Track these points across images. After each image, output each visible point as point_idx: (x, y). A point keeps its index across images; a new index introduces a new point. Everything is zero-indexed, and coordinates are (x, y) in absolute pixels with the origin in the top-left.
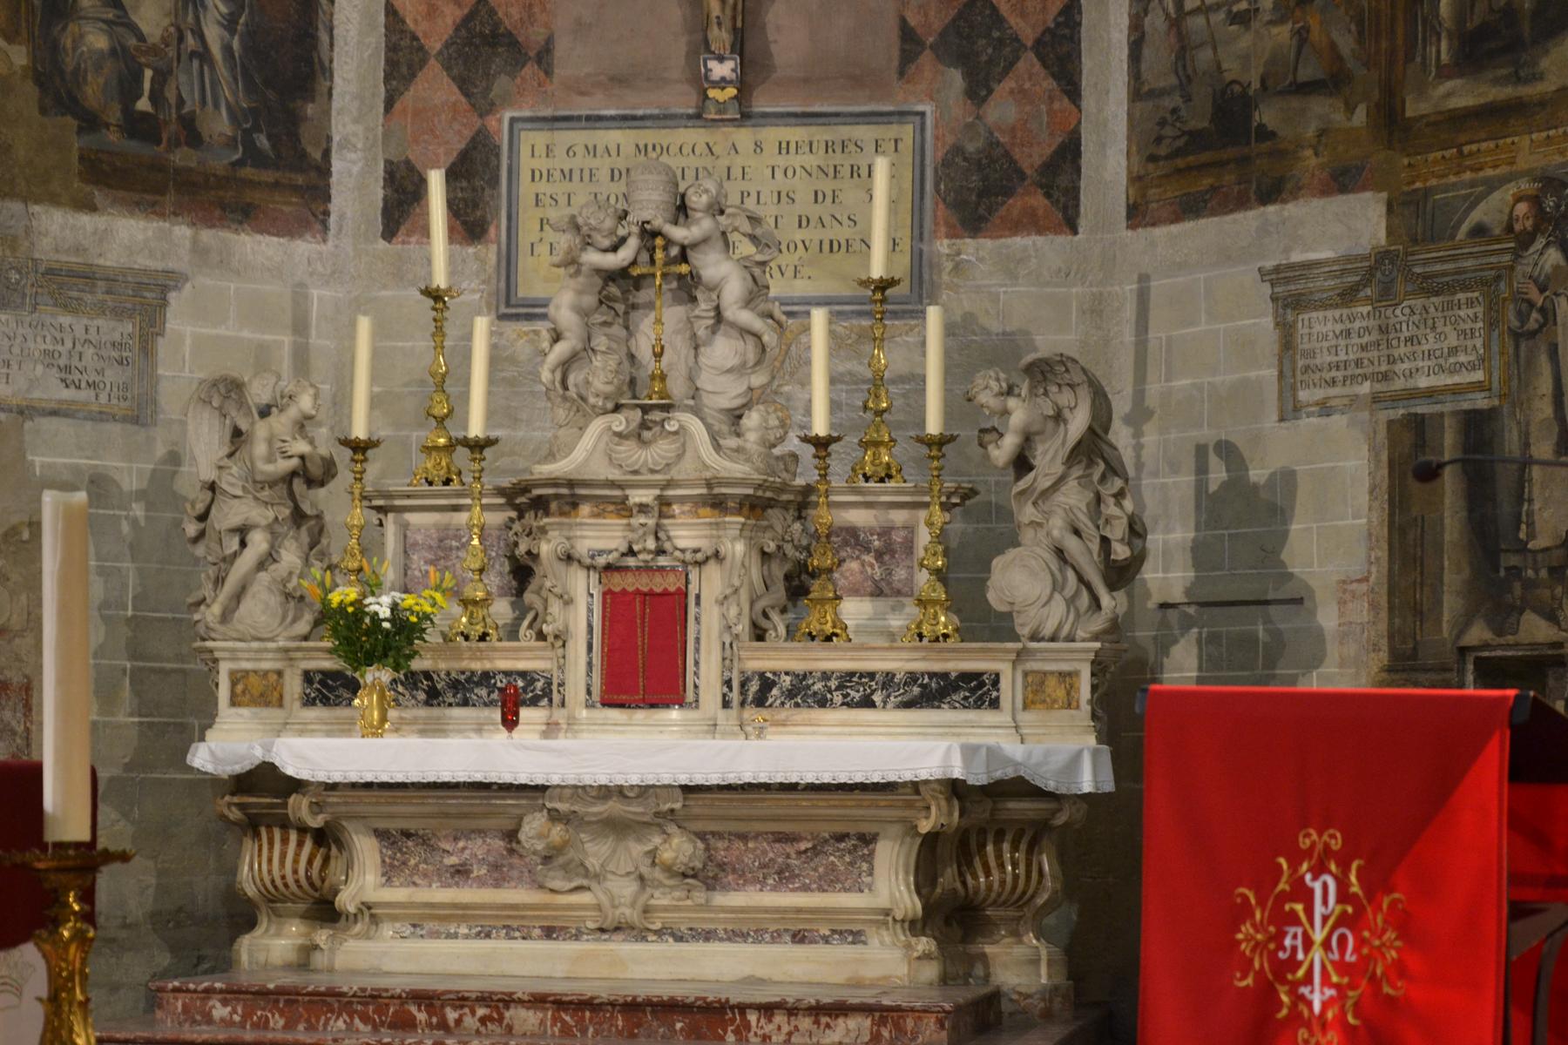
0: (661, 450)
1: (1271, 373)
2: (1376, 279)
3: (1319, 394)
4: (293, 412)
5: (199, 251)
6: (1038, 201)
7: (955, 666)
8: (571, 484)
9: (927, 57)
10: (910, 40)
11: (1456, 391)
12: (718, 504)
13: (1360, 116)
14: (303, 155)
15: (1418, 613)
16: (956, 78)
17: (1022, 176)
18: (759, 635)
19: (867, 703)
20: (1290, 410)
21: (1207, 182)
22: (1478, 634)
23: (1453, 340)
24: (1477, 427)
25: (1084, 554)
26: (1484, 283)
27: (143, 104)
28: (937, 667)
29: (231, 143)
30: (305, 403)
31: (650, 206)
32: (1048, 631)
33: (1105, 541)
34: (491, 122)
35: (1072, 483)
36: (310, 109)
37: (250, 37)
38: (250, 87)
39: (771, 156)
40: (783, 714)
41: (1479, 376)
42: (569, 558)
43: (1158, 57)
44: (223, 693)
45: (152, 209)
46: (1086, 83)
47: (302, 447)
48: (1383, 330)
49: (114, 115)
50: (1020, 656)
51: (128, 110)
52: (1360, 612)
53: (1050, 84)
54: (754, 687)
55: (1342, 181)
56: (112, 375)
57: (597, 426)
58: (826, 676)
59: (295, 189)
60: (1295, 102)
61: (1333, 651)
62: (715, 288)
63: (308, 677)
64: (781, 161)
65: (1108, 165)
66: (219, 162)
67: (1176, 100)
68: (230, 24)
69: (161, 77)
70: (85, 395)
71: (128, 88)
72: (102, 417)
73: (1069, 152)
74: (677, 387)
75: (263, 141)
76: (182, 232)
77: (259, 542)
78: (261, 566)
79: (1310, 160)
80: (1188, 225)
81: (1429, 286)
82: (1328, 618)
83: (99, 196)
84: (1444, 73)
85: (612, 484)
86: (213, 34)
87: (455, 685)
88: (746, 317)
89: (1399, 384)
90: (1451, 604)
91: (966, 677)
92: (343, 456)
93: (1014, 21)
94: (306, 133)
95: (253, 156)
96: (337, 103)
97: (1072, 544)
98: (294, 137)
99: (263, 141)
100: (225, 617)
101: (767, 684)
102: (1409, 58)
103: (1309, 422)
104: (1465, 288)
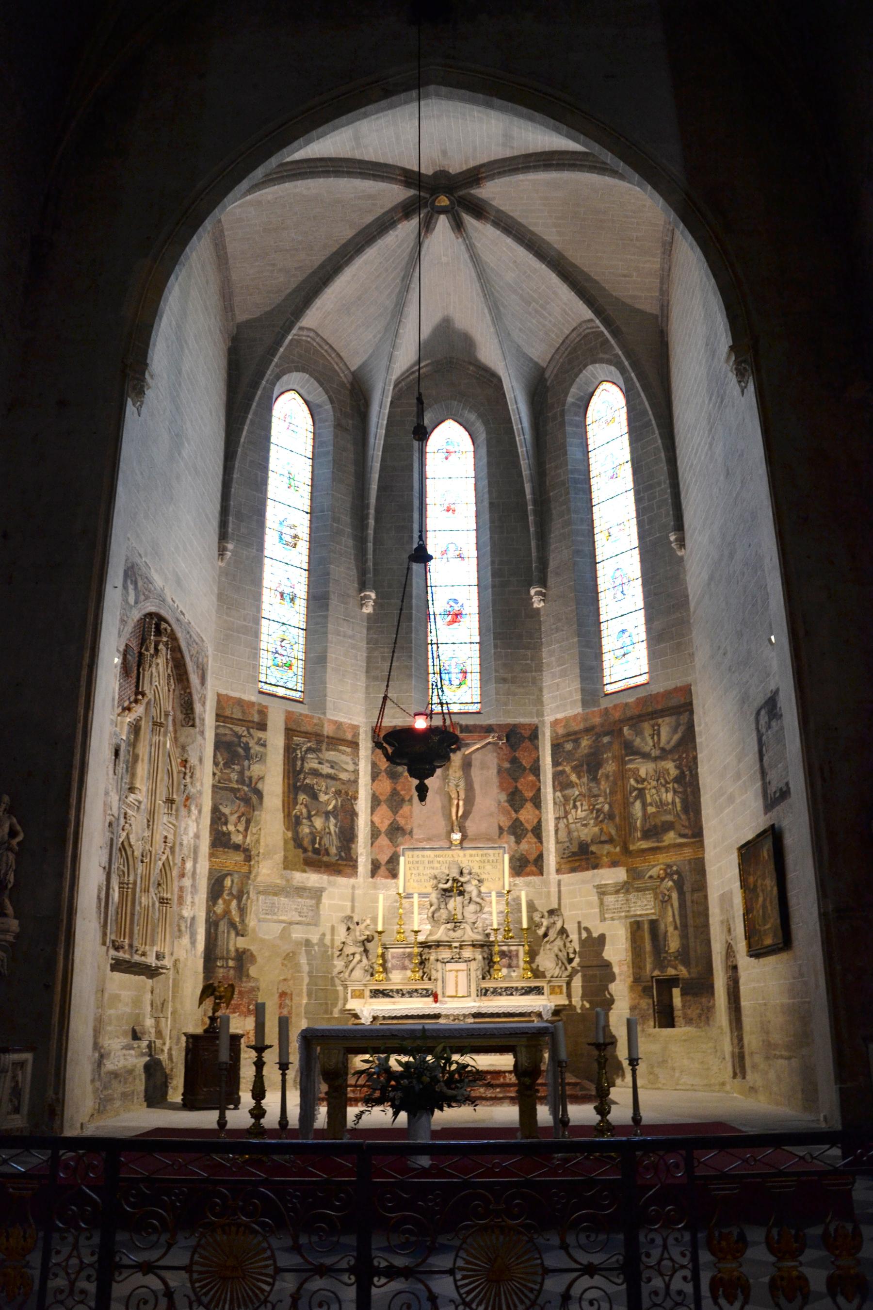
0: (459, 933)
1: (597, 910)
2: (625, 888)
3: (611, 915)
4: (365, 924)
5: (329, 882)
6: (534, 869)
7: (533, 985)
8: (438, 942)
9: (505, 833)
10: (500, 828)
11: (647, 915)
12: (474, 946)
13: (618, 849)
14: (352, 858)
15: (640, 968)
16: (512, 838)
17: (529, 862)
18: (484, 978)
19: (511, 994)
20: (603, 919)
21: (577, 864)
22: (656, 973)
23: (645, 903)
24: (654, 924)
25: (563, 955)
26: (653, 889)
27: (317, 846)
28: (529, 985)
29: (336, 855)
30: (368, 922)
31: (455, 874)
32: (555, 975)
33: (568, 953)
34: (398, 849)
35: (558, 939)
36: (353, 846)
37: (340, 828)
38: (340, 841)
39: (468, 857)
40: (491, 998)
41: (653, 911)
42: (437, 960)
43: (563, 834)
44: (349, 995)
45: (319, 872)
46: (544, 839)
47: (368, 933)
48: (627, 900)
49: (310, 848)
50: (550, 981)
51: (313, 847)
52: (625, 968)
53: (535, 840)
54: (484, 991)
55: (614, 864)
56: (310, 914)
57: (443, 927)
58: (501, 988)
59: (350, 866)
60: (600, 846)
61: (618, 978)
62: (469, 893)
63: (371, 991)
64: (471, 859)
65: (551, 860)
66: (334, 859)
67: (568, 844)
68: (336, 825)
69: (321, 839)
70: (304, 919)
71: (313, 842)
72: (308, 924)
73: (540, 857)
74: (459, 917)
75: (343, 854)
76: (325, 877)
77: (357, 957)
78: (358, 963)
79: (605, 859)
80: (573, 874)
81: (638, 890)
82: (616, 970)
83: (307, 868)
84: (639, 840)
85: (448, 942)
86: (332, 828)
87: (409, 993)
88: (478, 900)
89: (632, 913)
90: (649, 967)
91: (536, 987)
92: (376, 935)
93: (526, 825)
94: (352, 851)
95: (341, 858)
96: (359, 844)
97: (560, 954)
98: (350, 854)
99: (343, 854)
100: (349, 976)
101: (487, 991)
102: (630, 835)
103: (608, 922)
104: (648, 890)
